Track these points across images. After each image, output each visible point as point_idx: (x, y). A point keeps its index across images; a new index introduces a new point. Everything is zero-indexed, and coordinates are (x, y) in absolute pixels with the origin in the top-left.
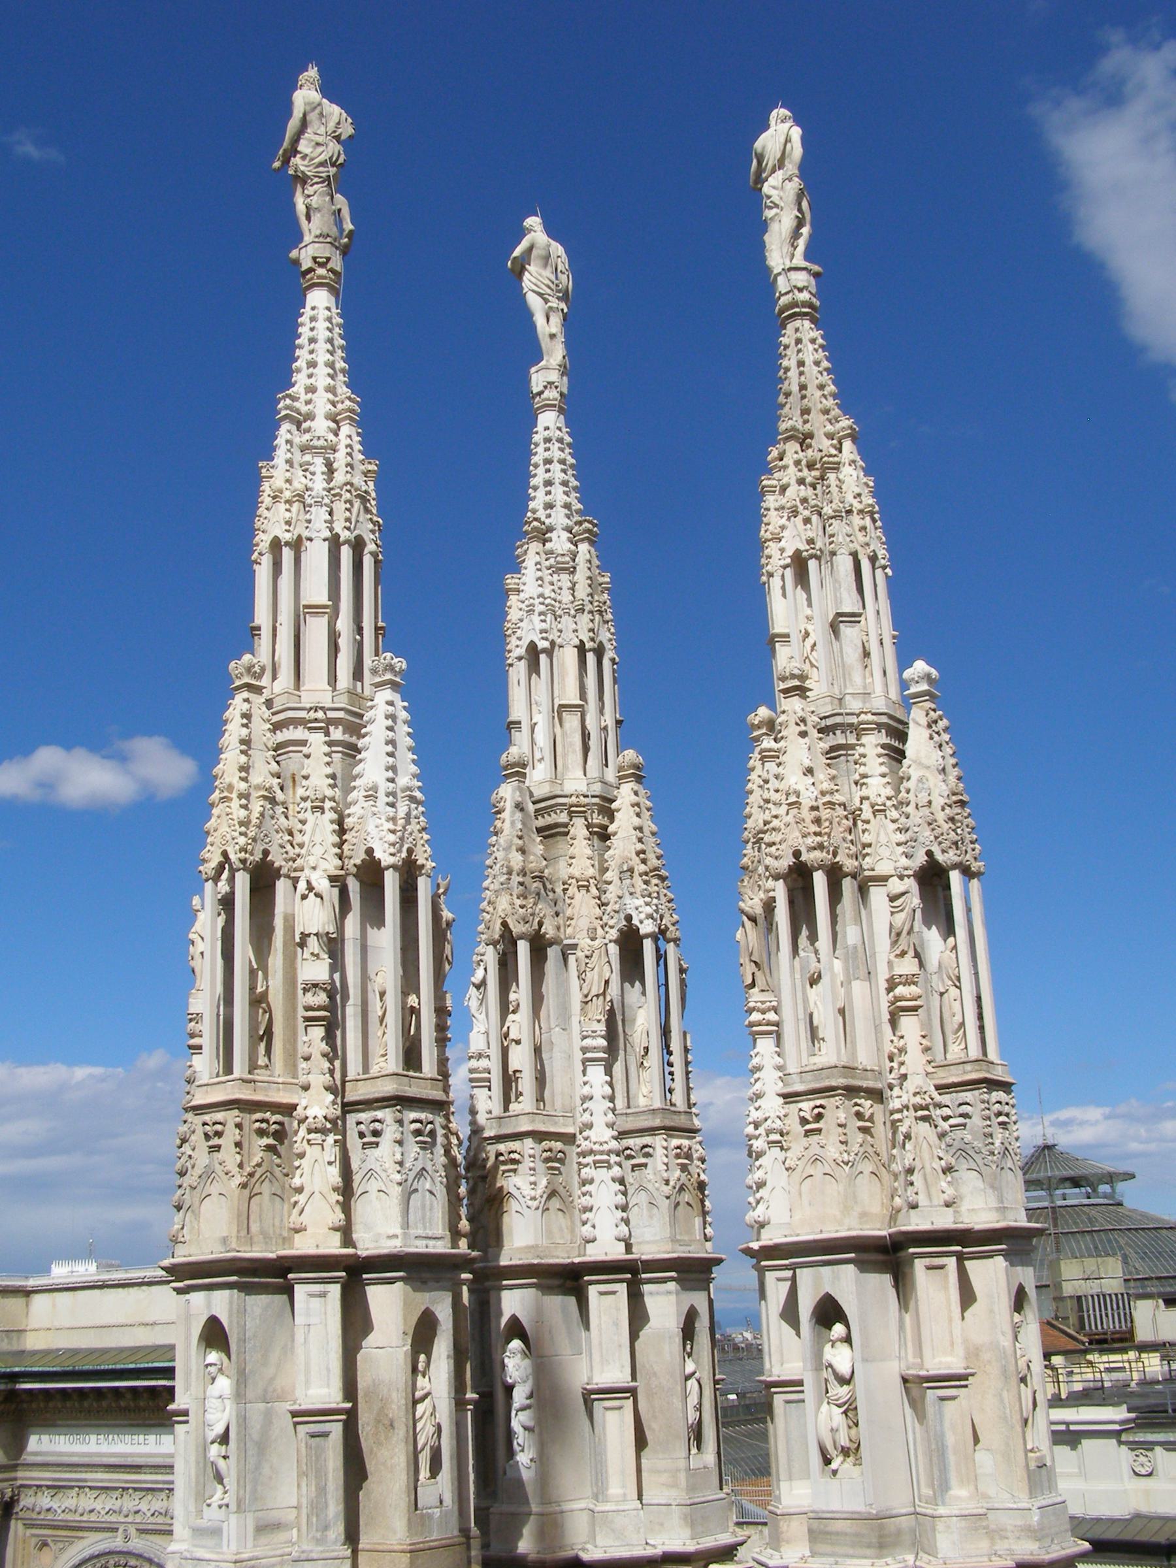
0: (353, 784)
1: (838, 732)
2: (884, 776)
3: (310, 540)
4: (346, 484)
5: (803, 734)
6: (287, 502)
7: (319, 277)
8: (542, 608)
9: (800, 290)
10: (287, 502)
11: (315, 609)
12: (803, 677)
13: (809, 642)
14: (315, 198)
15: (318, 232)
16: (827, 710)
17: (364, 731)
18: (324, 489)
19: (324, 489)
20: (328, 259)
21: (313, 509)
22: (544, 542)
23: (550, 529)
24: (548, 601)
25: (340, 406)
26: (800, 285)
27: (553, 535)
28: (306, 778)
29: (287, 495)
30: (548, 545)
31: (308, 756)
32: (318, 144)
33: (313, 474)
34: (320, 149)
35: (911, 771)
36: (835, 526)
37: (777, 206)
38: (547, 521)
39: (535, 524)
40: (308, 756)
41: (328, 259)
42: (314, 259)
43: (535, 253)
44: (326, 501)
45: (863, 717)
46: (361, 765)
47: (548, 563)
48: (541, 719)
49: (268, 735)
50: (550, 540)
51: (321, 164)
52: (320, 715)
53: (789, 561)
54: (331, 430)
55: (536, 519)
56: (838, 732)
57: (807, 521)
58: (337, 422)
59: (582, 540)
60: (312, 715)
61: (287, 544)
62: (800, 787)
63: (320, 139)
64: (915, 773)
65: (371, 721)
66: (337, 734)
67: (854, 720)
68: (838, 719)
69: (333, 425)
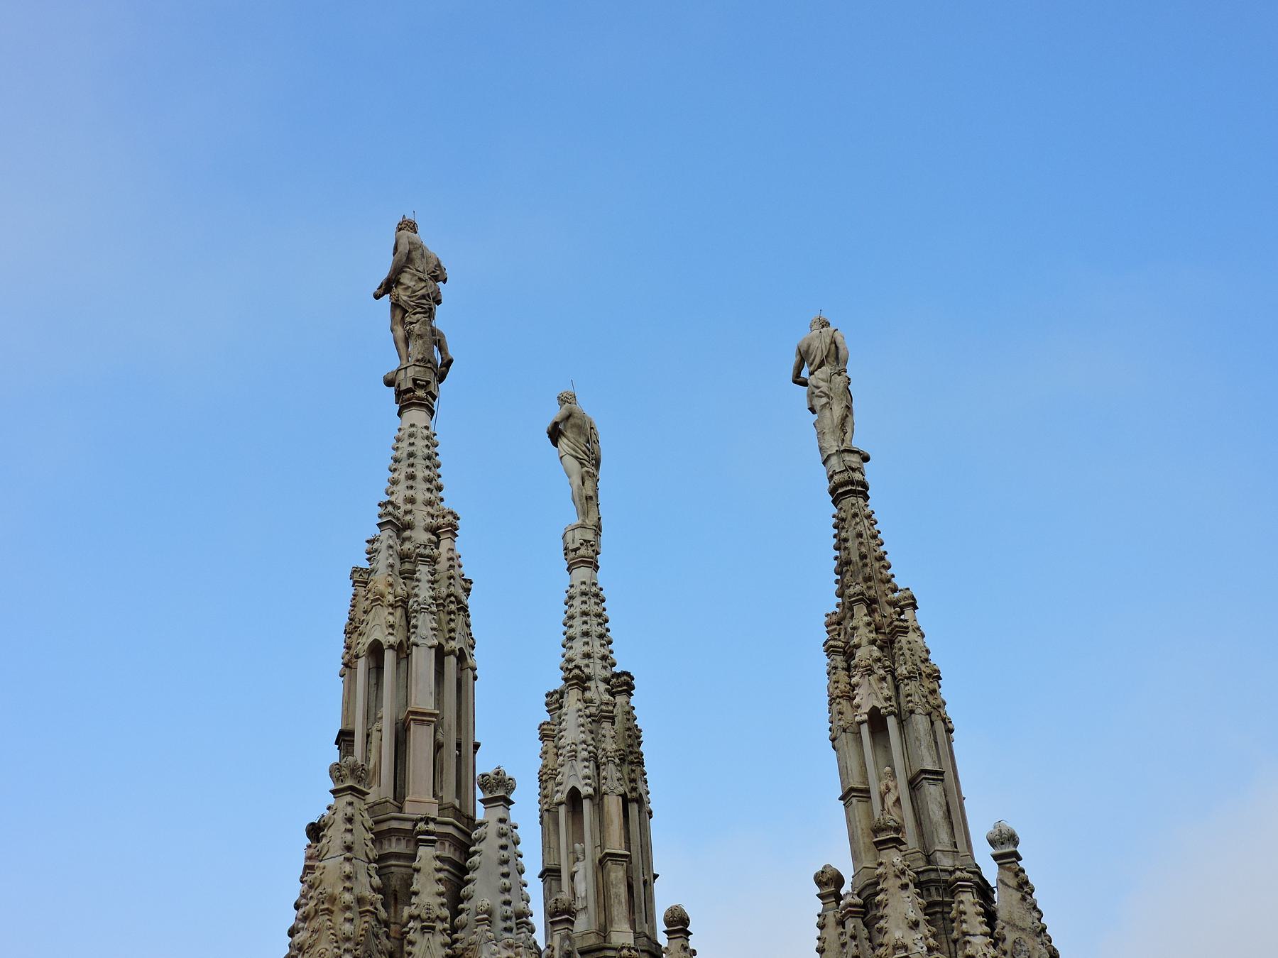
0: (461, 906)
1: (933, 890)
2: (985, 935)
3: (417, 645)
4: (449, 596)
5: (904, 887)
6: (391, 605)
7: (418, 398)
8: (585, 754)
9: (854, 470)
10: (391, 605)
11: (421, 717)
12: (898, 829)
13: (890, 799)
14: (417, 326)
15: (420, 357)
16: (921, 865)
17: (472, 849)
18: (431, 597)
19: (431, 597)
20: (428, 383)
21: (421, 616)
22: (585, 689)
23: (589, 678)
24: (591, 748)
25: (441, 521)
26: (854, 466)
27: (591, 684)
28: (416, 894)
29: (391, 598)
30: (588, 695)
31: (418, 870)
32: (421, 280)
33: (418, 580)
34: (423, 284)
35: (1005, 932)
36: (911, 687)
37: (828, 396)
38: (586, 670)
39: (577, 671)
40: (418, 870)
41: (428, 383)
42: (414, 380)
43: (572, 421)
44: (434, 609)
45: (958, 874)
46: (470, 886)
47: (587, 712)
48: (584, 871)
49: (370, 844)
50: (589, 689)
51: (423, 297)
52: (431, 826)
53: (865, 717)
54: (430, 541)
55: (577, 667)
56: (933, 890)
57: (884, 679)
58: (438, 537)
59: (620, 693)
60: (422, 826)
61: (391, 647)
62: (908, 941)
63: (422, 276)
64: (1011, 936)
65: (481, 840)
66: (448, 852)
67: (945, 877)
68: (933, 876)
69: (434, 538)
